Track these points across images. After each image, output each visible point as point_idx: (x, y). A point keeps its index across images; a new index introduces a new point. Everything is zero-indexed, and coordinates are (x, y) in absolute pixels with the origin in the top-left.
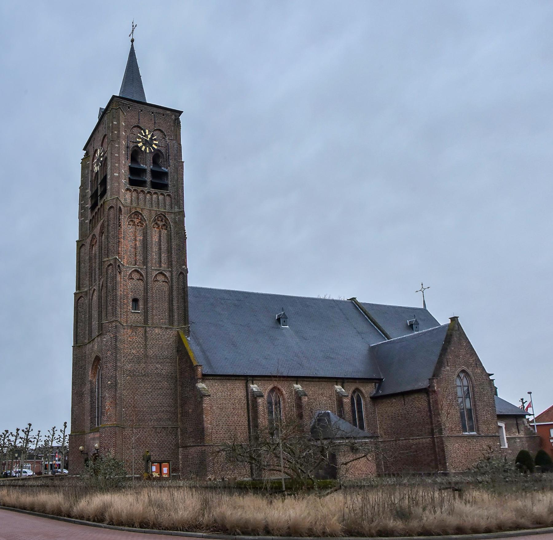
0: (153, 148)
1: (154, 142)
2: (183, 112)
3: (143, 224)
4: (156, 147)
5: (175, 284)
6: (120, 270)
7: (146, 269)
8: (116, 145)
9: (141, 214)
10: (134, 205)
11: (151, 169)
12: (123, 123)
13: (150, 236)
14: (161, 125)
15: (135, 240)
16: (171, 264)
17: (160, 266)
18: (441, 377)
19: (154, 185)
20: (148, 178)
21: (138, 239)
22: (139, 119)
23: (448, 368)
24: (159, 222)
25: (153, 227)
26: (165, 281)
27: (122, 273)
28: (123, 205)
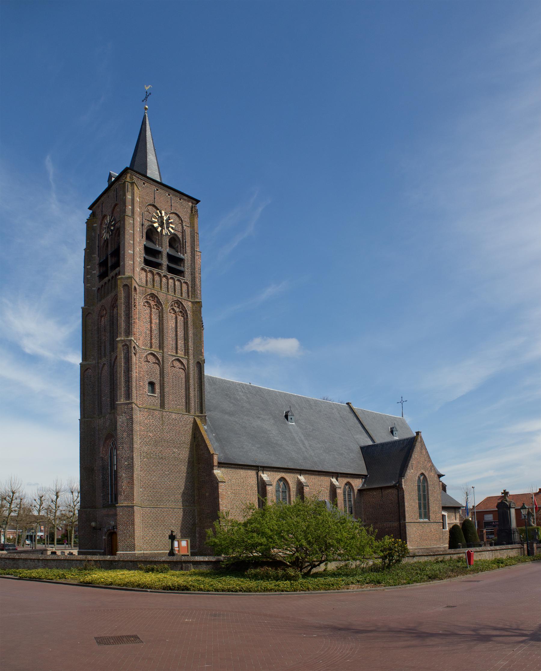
0: (169, 231)
1: (171, 225)
2: (200, 201)
3: (159, 308)
4: (173, 231)
5: (192, 372)
6: (136, 351)
7: (163, 353)
8: (131, 221)
9: (157, 297)
10: (150, 285)
11: (167, 253)
12: (138, 199)
13: (167, 321)
14: (177, 209)
15: (151, 322)
16: (188, 353)
17: (177, 353)
18: (407, 478)
19: (170, 270)
20: (165, 262)
21: (153, 321)
22: (155, 198)
23: (412, 471)
24: (175, 308)
25: (170, 312)
26: (181, 368)
27: (138, 354)
28: (138, 285)
